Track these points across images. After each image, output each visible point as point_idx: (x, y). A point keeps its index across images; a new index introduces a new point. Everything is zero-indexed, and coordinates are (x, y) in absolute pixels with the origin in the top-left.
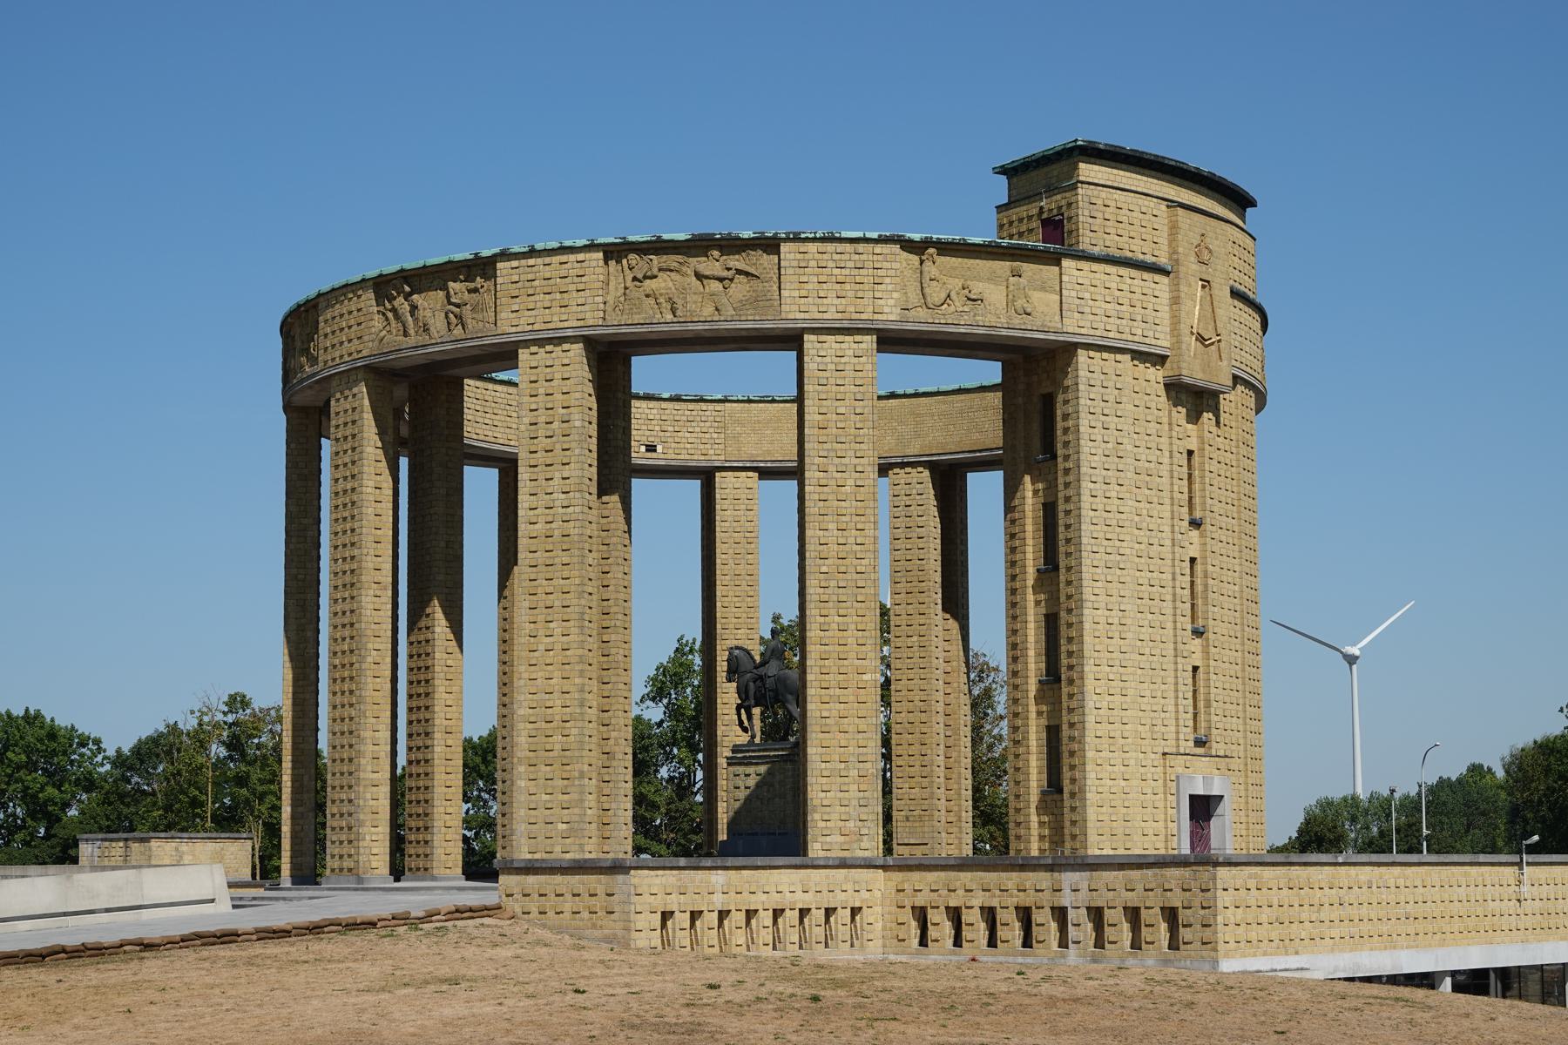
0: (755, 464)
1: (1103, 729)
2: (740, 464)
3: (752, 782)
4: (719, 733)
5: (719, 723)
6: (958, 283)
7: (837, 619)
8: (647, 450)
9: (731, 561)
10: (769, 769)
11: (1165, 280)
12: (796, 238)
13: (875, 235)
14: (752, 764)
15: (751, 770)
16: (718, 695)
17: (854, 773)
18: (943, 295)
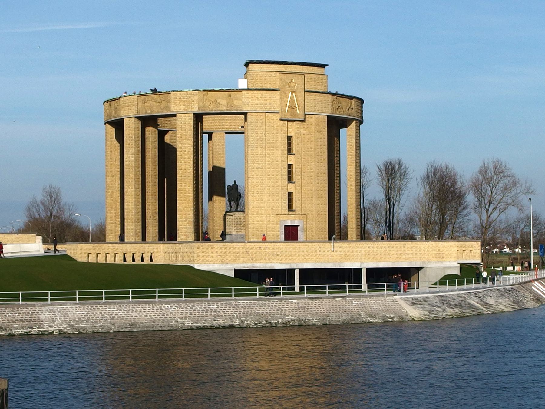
1: (286, 209)
6: (213, 100)
7: (184, 184)
8: (241, 128)
11: (278, 93)
12: (174, 91)
13: (191, 90)
17: (187, 221)
18: (209, 104)
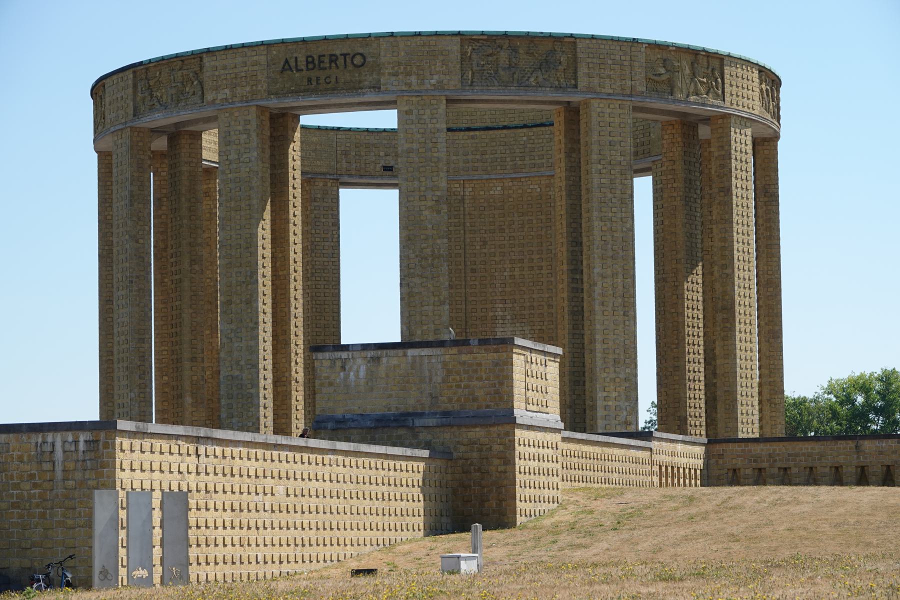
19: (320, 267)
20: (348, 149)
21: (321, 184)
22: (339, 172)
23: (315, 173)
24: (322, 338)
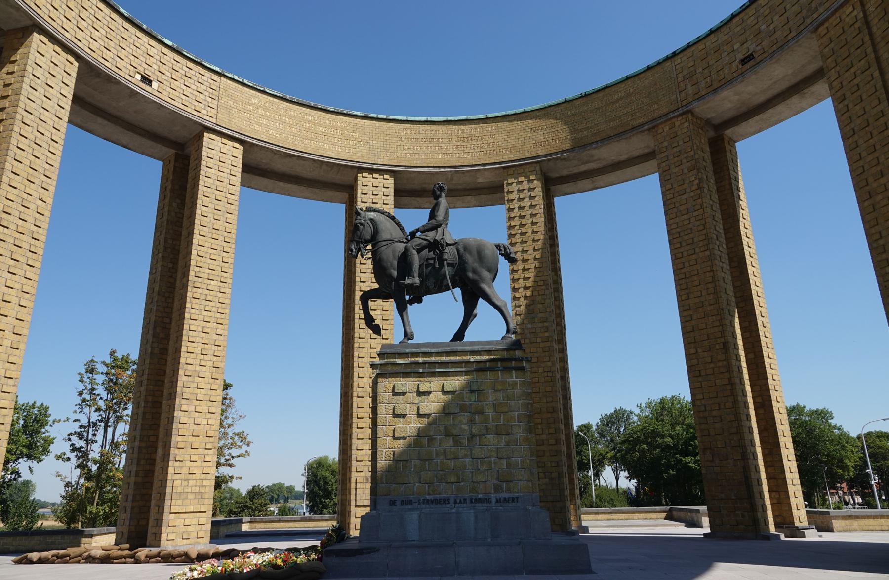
0: (242, 137)
2: (230, 133)
3: (433, 404)
4: (180, 383)
5: (181, 372)
9: (211, 215)
10: (469, 384)
14: (433, 374)
15: (432, 384)
16: (183, 343)
19: (678, 230)
20: (692, 69)
21: (666, 129)
22: (684, 103)
23: (653, 120)
24: (694, 323)
